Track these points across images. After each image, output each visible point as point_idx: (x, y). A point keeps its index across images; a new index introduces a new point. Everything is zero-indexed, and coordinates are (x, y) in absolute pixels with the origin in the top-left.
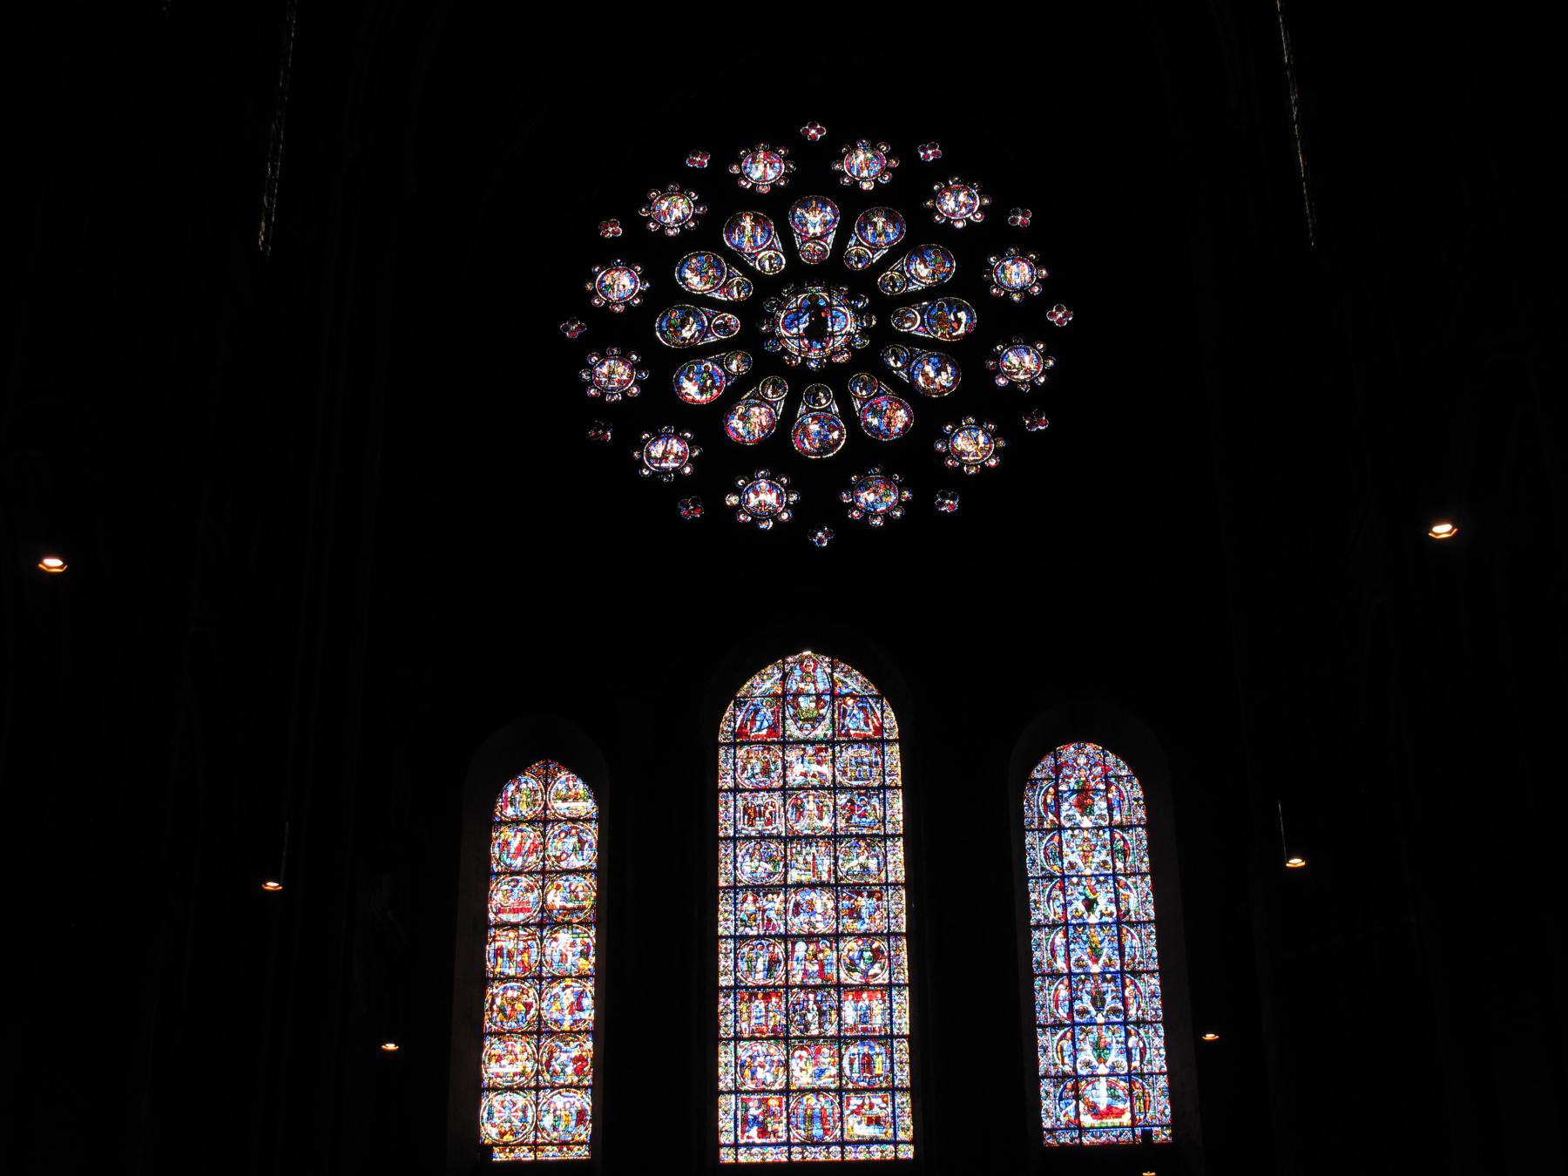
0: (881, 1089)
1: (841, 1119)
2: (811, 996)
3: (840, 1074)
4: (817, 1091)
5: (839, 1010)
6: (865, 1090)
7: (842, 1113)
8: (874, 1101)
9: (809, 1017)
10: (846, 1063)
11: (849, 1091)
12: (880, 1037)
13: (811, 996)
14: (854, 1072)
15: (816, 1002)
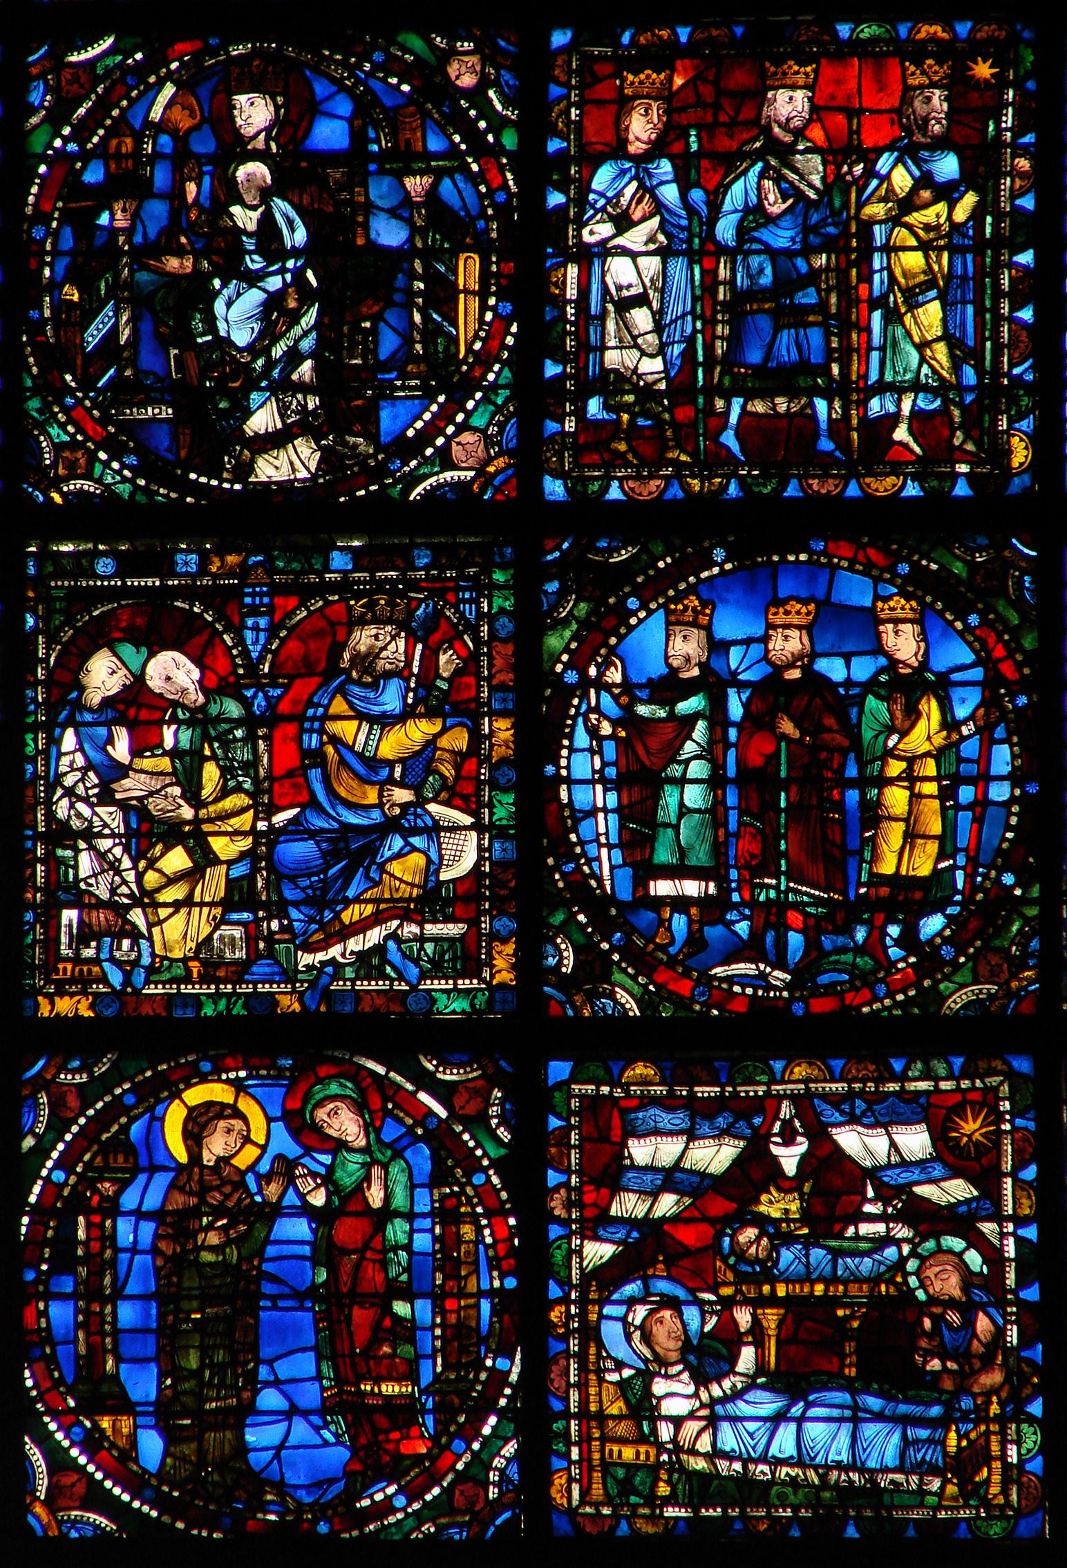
0: (925, 1033)
1: (524, 1320)
2: (254, 113)
3: (531, 873)
4: (294, 1045)
5: (533, 246)
6: (763, 1032)
7: (533, 1260)
8: (859, 1143)
9: (237, 316)
10: (583, 769)
11: (608, 1043)
12: (934, 520)
13: (254, 113)
14: (661, 841)
15: (296, 170)
